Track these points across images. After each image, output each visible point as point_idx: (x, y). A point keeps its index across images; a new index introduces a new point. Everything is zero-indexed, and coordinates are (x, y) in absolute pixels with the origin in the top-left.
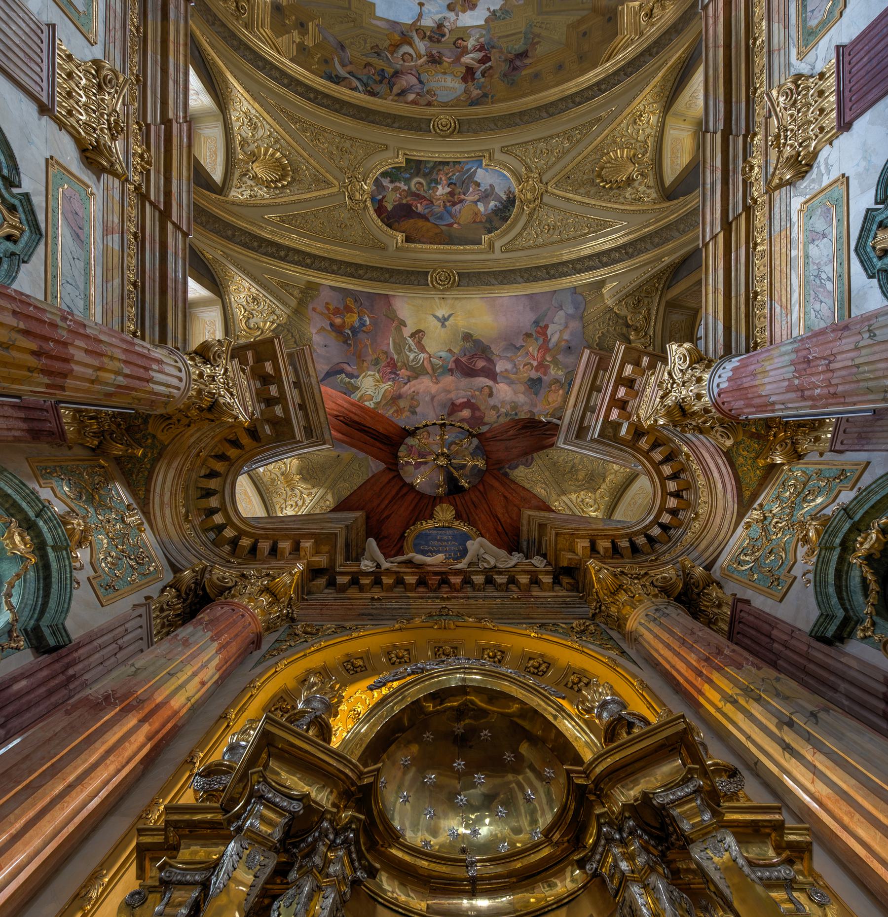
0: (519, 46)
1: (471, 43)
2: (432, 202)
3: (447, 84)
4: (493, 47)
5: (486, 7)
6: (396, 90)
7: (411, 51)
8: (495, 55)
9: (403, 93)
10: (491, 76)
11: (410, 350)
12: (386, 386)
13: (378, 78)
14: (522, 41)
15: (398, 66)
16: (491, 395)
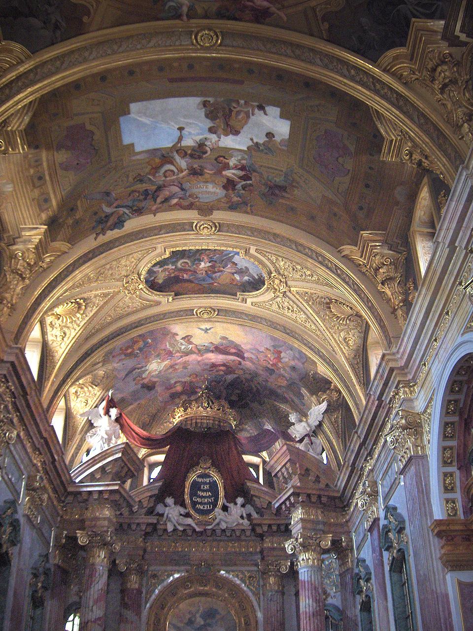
0: (279, 180)
1: (232, 162)
2: (195, 272)
3: (208, 190)
4: (255, 171)
5: (250, 136)
6: (159, 200)
7: (172, 167)
8: (255, 178)
9: (167, 200)
10: (251, 191)
11: (182, 344)
12: (167, 362)
13: (142, 197)
14: (282, 178)
15: (161, 183)
16: (240, 363)
